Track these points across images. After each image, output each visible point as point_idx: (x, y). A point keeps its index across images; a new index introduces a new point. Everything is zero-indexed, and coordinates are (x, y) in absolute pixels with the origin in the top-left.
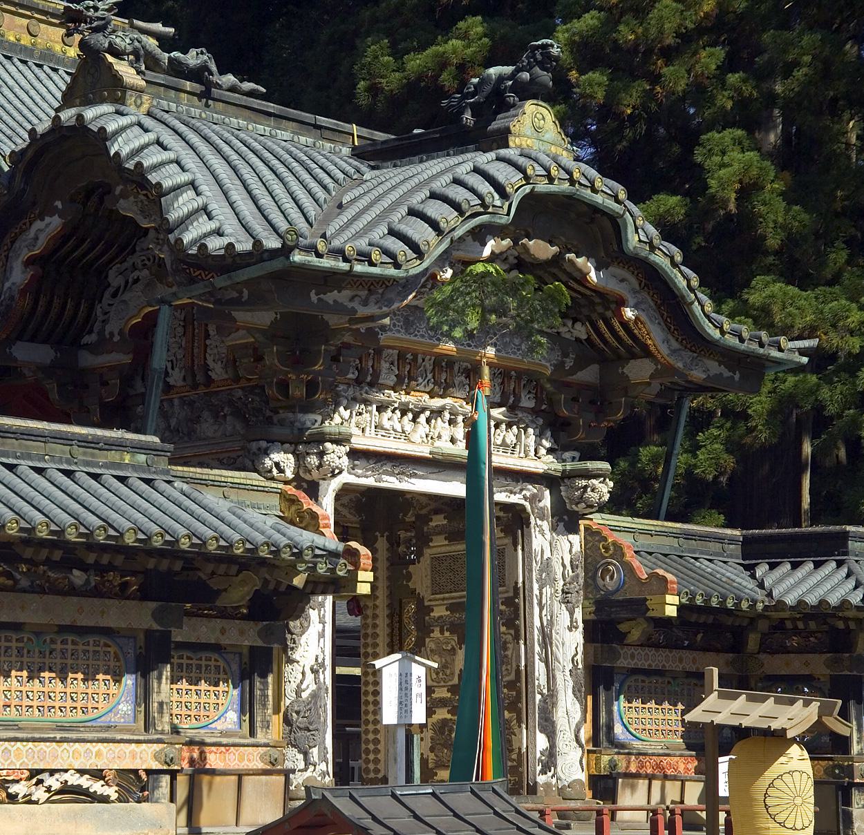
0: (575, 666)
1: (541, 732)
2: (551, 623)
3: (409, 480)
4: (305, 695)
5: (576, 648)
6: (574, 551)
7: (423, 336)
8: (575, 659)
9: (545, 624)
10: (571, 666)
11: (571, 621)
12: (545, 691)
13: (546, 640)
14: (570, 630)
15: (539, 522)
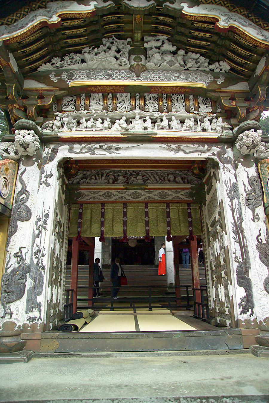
0: (260, 243)
1: (240, 286)
2: (241, 219)
3: (117, 152)
4: (9, 271)
5: (260, 231)
6: (250, 176)
7: (101, 79)
8: (259, 238)
9: (236, 220)
10: (256, 242)
11: (253, 215)
12: (241, 260)
13: (239, 230)
14: (254, 221)
15: (226, 165)
